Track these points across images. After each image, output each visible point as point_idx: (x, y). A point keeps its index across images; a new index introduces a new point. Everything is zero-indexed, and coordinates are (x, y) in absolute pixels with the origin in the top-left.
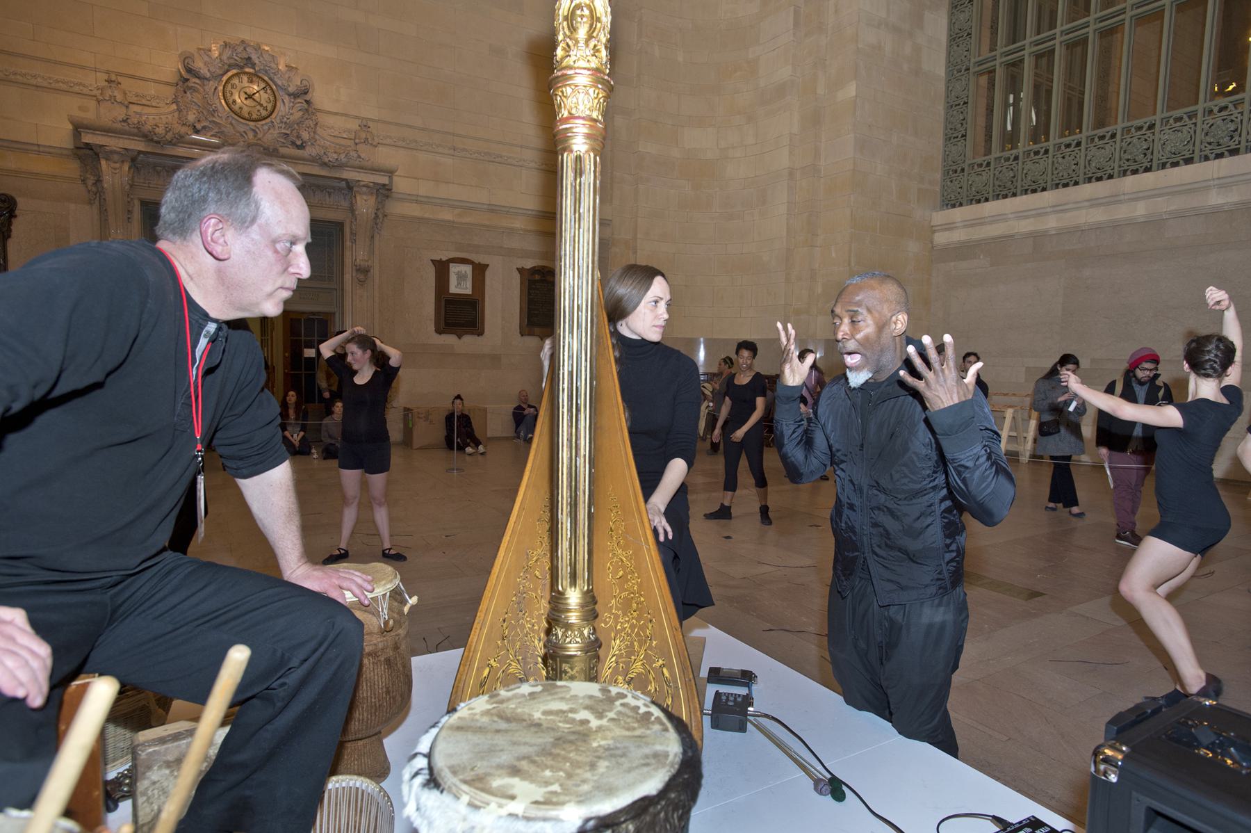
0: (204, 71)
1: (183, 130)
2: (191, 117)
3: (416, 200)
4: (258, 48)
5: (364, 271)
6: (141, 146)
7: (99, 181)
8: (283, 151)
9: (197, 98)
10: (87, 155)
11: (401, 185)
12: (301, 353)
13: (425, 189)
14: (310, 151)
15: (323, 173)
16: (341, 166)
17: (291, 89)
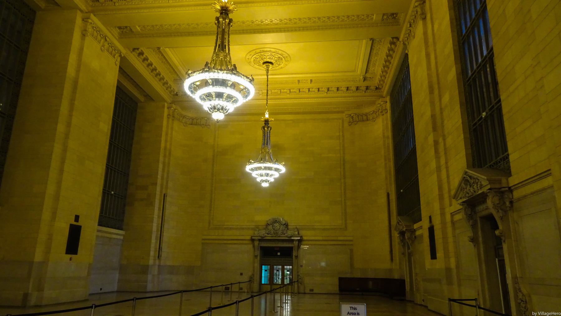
5: (297, 257)
6: (260, 238)
11: (305, 238)
16: (291, 237)
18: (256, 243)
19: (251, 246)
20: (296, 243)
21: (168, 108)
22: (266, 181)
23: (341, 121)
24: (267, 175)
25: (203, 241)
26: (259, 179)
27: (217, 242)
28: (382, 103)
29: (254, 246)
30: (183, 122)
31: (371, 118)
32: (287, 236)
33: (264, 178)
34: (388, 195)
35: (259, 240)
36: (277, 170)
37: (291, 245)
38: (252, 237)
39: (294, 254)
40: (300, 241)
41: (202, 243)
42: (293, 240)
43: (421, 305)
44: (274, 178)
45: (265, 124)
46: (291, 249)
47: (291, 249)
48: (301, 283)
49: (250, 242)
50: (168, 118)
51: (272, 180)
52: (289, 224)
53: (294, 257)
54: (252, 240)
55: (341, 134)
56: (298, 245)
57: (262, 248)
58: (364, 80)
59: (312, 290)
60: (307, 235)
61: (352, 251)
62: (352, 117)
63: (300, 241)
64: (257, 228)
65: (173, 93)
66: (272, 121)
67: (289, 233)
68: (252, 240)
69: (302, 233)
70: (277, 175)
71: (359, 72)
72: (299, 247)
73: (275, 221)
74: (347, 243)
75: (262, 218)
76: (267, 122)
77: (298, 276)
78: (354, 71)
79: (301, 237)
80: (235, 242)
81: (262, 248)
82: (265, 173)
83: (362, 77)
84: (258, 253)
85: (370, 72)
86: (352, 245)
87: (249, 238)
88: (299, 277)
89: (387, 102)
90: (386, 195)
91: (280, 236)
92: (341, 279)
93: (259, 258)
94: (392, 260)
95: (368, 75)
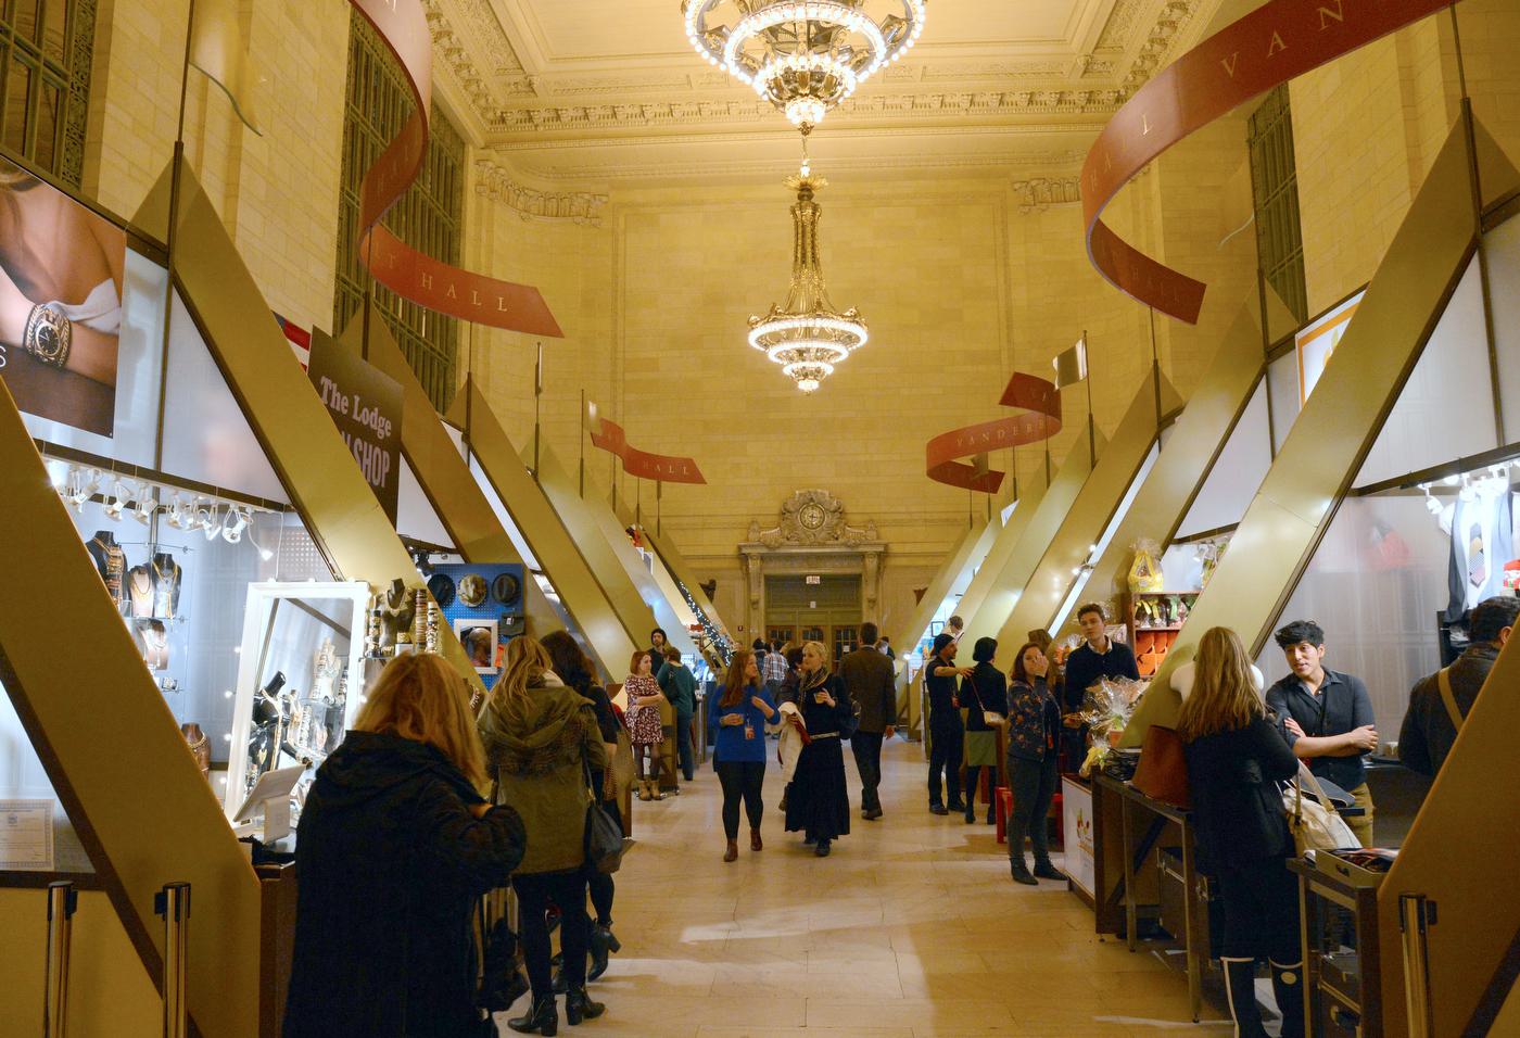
0: (792, 509)
1: (782, 540)
2: (786, 533)
3: (904, 555)
4: (816, 493)
5: (873, 602)
6: (764, 551)
7: (747, 566)
8: (828, 542)
9: (788, 522)
10: (743, 558)
11: (895, 548)
12: (841, 650)
13: (908, 549)
14: (841, 540)
15: (849, 550)
16: (857, 546)
17: (832, 509)
18: (754, 566)
20: (872, 564)
21: (477, 163)
24: (822, 355)
30: (520, 206)
32: (845, 545)
33: (811, 365)
35: (762, 558)
36: (849, 339)
37: (856, 571)
38: (740, 548)
39: (868, 591)
40: (883, 556)
42: (862, 556)
44: (835, 365)
45: (801, 197)
46: (855, 581)
47: (855, 581)
49: (736, 564)
50: (479, 194)
51: (828, 369)
52: (849, 509)
56: (879, 568)
57: (770, 581)
58: (1085, 72)
62: (1033, 191)
64: (752, 524)
65: (490, 115)
66: (822, 187)
69: (889, 535)
70: (844, 353)
71: (1075, 45)
72: (879, 571)
73: (810, 501)
76: (805, 191)
78: (1061, 41)
79: (886, 546)
81: (768, 579)
82: (810, 349)
83: (1081, 62)
84: (759, 593)
85: (1109, 42)
87: (732, 551)
91: (823, 545)
95: (1100, 58)
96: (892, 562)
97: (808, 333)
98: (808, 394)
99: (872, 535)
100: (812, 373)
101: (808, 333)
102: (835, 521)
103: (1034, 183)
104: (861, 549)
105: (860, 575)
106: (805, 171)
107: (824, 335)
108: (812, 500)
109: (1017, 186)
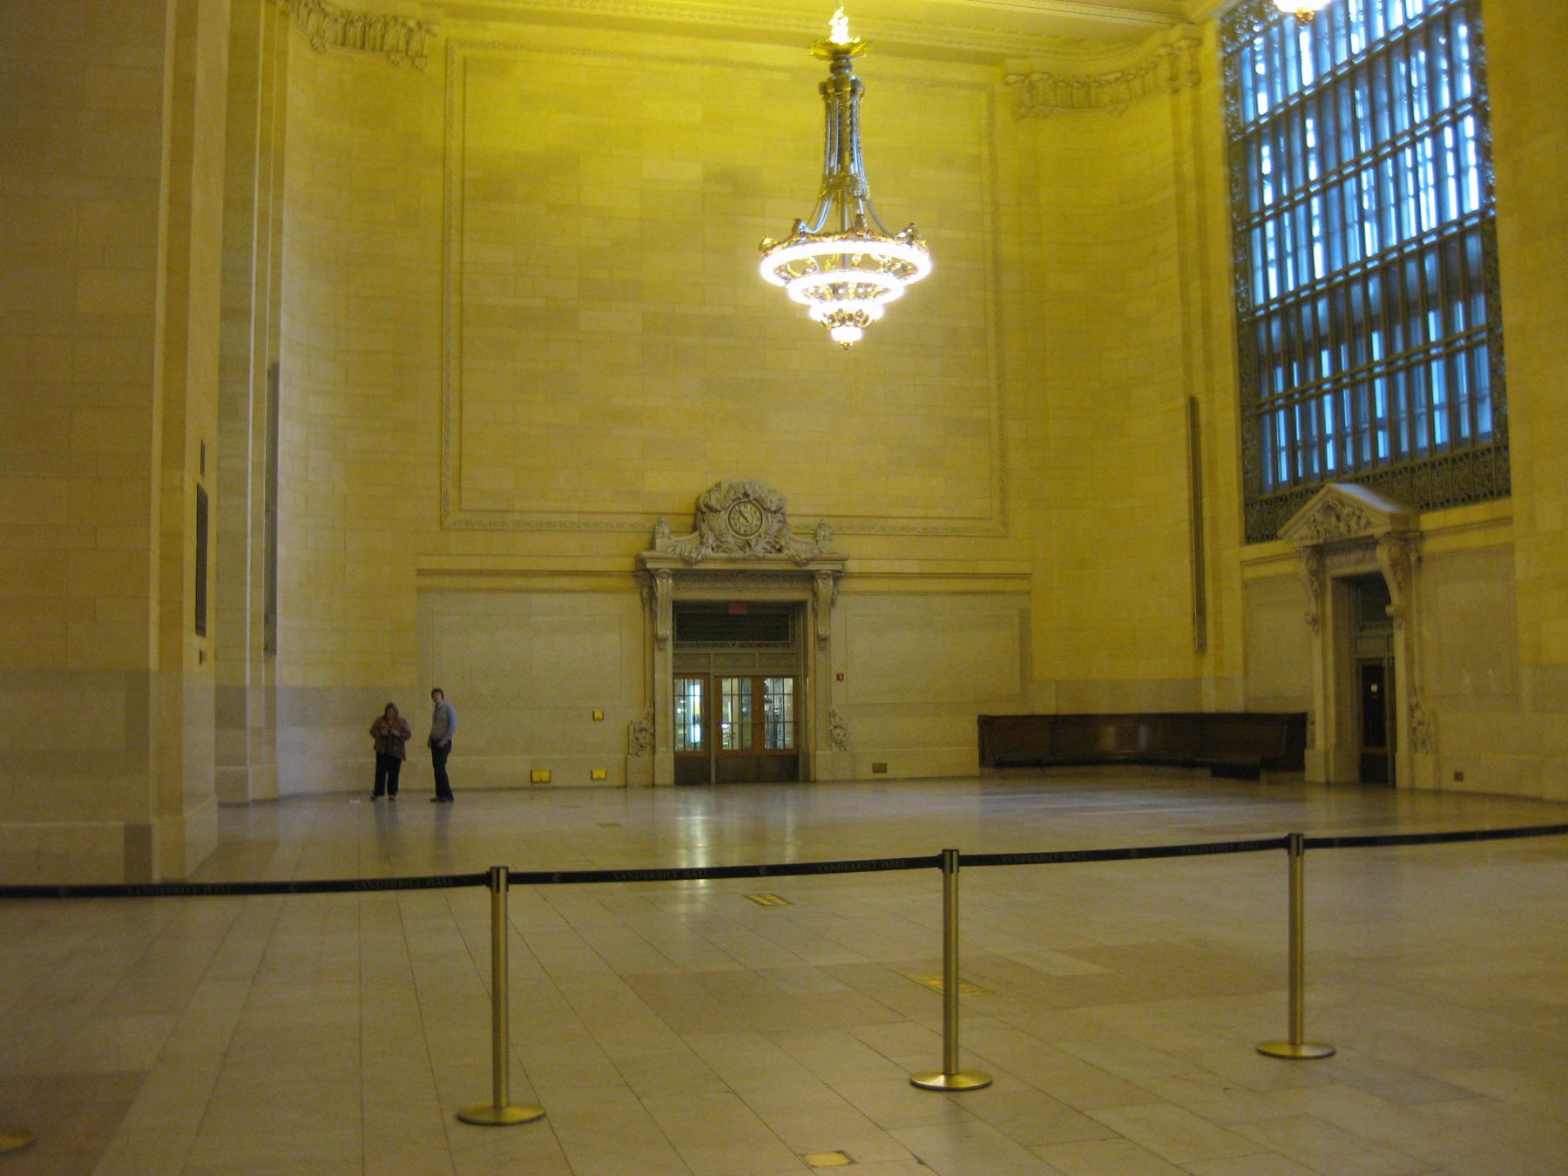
5: (823, 640)
6: (679, 566)
11: (852, 566)
18: (664, 587)
19: (632, 601)
22: (844, 319)
23: (983, 98)
25: (426, 581)
26: (819, 312)
27: (484, 582)
28: (1183, 43)
29: (650, 599)
31: (1106, 99)
33: (850, 306)
34: (1193, 404)
35: (677, 575)
38: (641, 561)
40: (837, 576)
41: (420, 590)
42: (810, 577)
43: (1438, 792)
48: (840, 744)
49: (630, 583)
52: (789, 510)
53: (811, 639)
54: (644, 575)
55: (985, 151)
59: (880, 768)
60: (862, 553)
61: (1025, 615)
63: (837, 576)
67: (799, 548)
68: (644, 575)
69: (840, 545)
74: (1010, 585)
75: (676, 484)
76: (839, 58)
77: (832, 715)
80: (564, 582)
84: (666, 628)
86: (1029, 593)
87: (627, 564)
88: (835, 721)
89: (1199, 42)
90: (1182, 402)
92: (987, 724)
93: (670, 643)
94: (1201, 646)
96: (846, 585)
97: (844, 262)
98: (846, 347)
99: (827, 547)
100: (851, 318)
101: (844, 262)
102: (776, 526)
103: (1035, 77)
104: (812, 567)
105: (801, 605)
106: (840, 35)
107: (868, 263)
108: (746, 495)
109: (1011, 79)
